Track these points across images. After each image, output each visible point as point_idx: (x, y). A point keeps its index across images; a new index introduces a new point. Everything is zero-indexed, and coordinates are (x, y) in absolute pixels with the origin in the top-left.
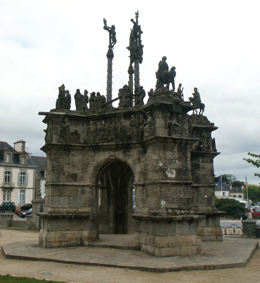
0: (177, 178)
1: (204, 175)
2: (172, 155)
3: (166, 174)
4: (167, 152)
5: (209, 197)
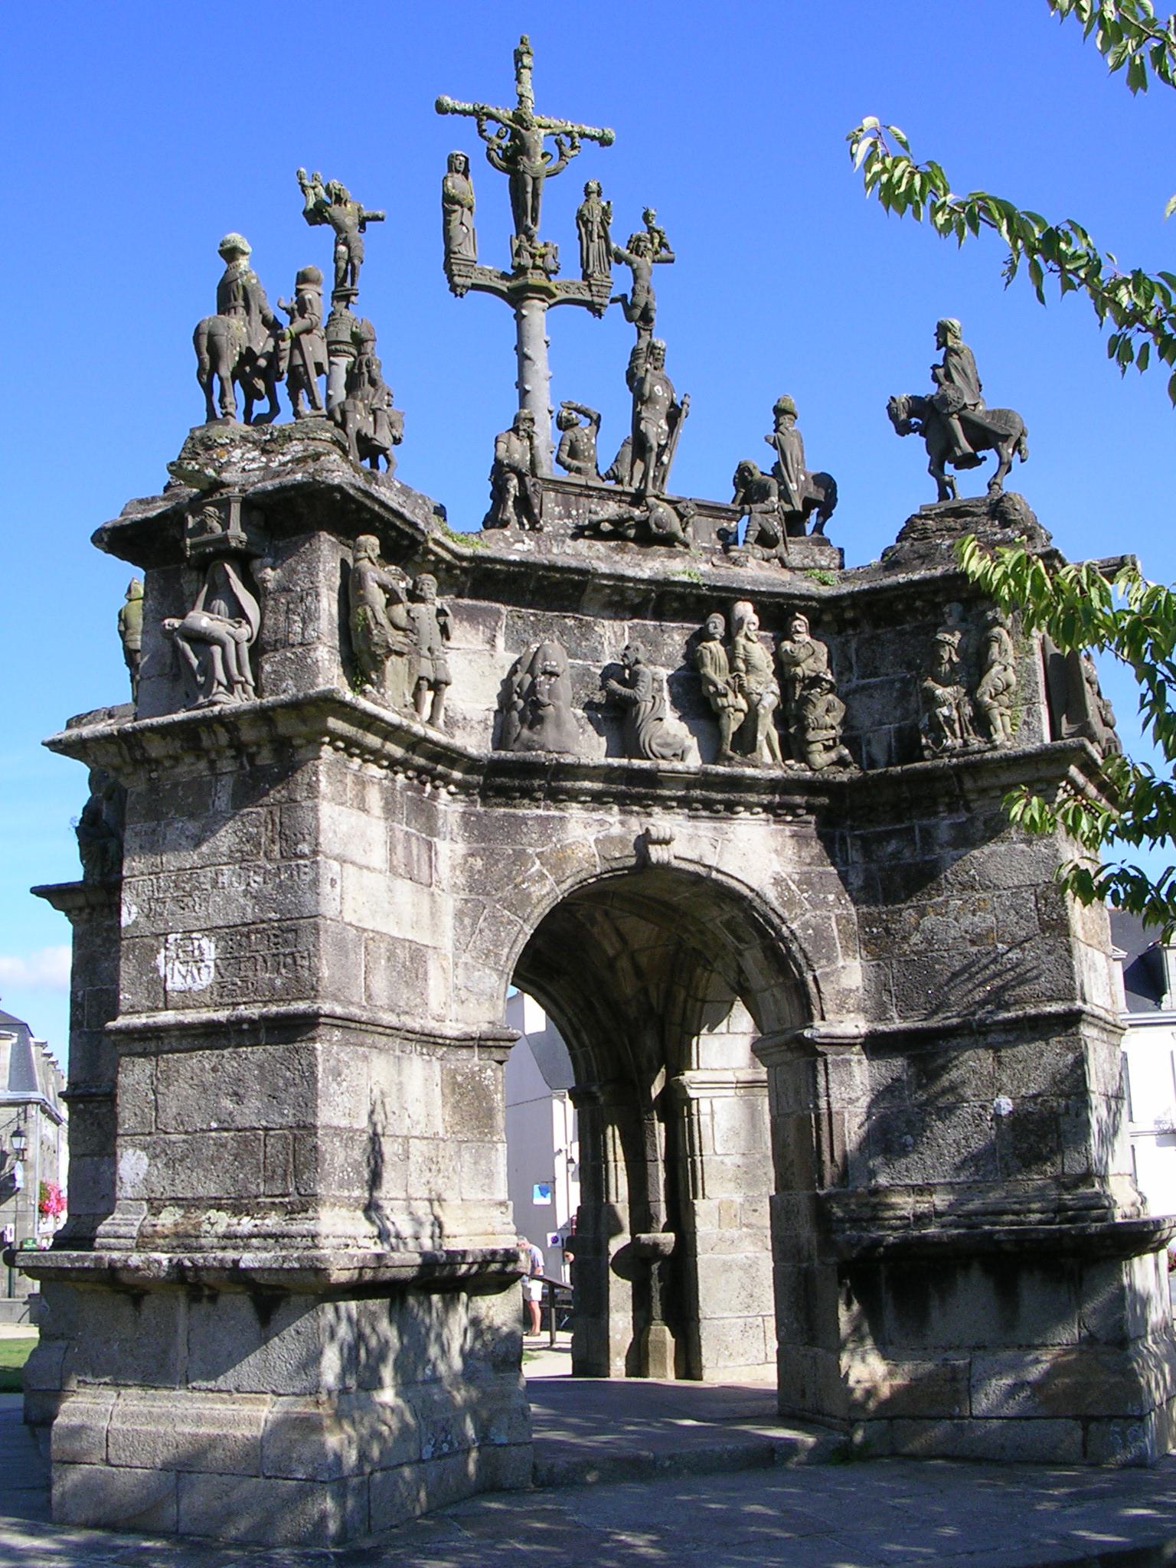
0: (223, 991)
1: (973, 942)
3: (156, 969)
4: (168, 825)
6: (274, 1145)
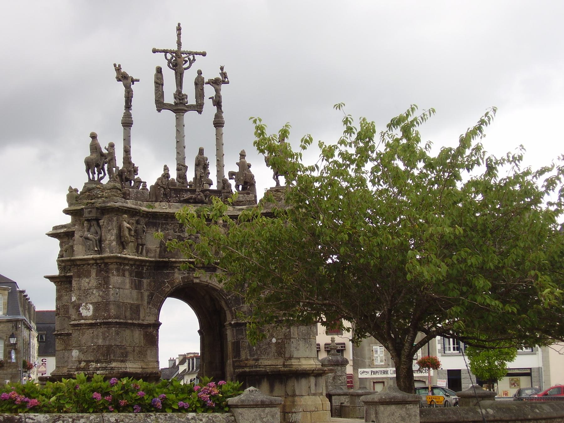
0: (94, 317)
2: (89, 283)
3: (80, 311)
5: (280, 341)
6: (105, 349)
